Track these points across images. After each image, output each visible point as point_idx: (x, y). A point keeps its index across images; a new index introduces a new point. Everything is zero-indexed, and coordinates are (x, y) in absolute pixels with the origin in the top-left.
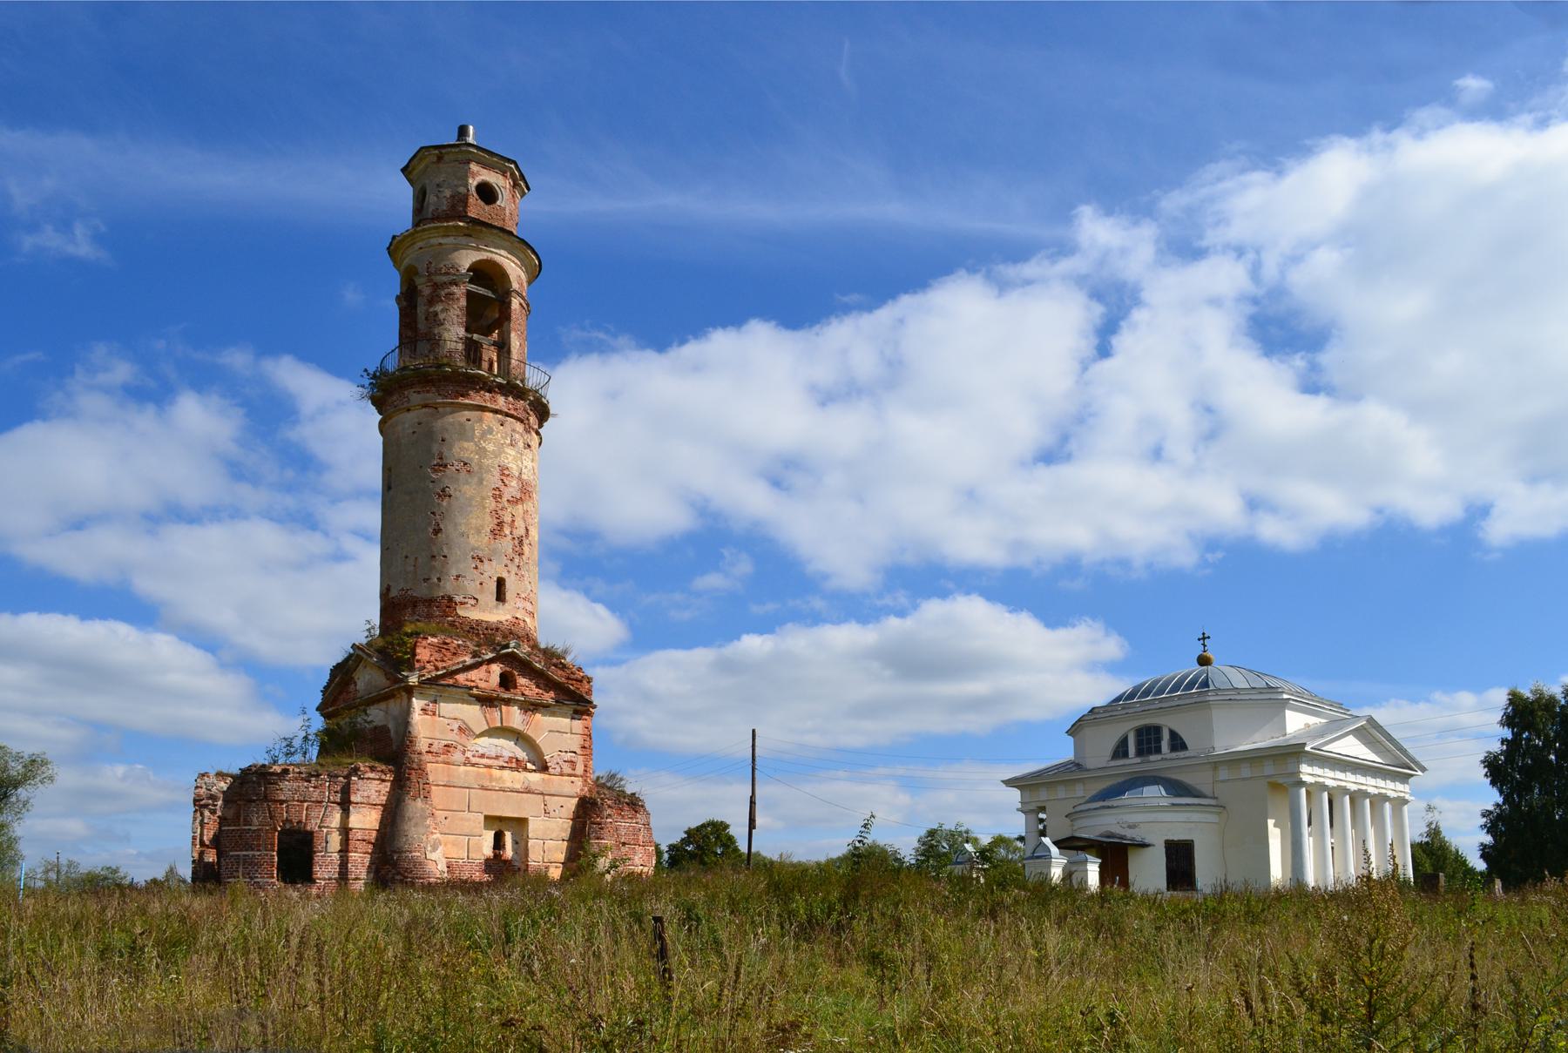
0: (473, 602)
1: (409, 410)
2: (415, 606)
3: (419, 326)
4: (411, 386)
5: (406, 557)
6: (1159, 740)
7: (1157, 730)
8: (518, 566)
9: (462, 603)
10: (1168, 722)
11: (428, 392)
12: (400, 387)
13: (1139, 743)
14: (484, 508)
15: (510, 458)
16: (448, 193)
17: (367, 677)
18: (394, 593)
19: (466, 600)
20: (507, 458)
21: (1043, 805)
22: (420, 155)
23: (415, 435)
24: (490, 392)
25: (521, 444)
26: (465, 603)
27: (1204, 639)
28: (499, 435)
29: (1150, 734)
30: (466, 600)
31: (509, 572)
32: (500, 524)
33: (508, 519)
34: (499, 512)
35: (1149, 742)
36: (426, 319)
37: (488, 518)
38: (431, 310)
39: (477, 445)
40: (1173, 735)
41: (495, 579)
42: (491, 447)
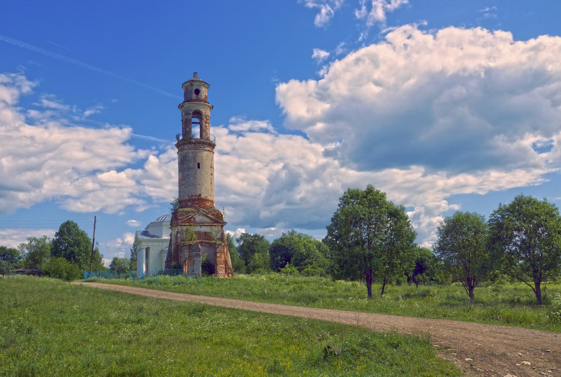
4: (206, 144)
11: (209, 147)
17: (201, 218)
21: (149, 247)
23: (207, 158)
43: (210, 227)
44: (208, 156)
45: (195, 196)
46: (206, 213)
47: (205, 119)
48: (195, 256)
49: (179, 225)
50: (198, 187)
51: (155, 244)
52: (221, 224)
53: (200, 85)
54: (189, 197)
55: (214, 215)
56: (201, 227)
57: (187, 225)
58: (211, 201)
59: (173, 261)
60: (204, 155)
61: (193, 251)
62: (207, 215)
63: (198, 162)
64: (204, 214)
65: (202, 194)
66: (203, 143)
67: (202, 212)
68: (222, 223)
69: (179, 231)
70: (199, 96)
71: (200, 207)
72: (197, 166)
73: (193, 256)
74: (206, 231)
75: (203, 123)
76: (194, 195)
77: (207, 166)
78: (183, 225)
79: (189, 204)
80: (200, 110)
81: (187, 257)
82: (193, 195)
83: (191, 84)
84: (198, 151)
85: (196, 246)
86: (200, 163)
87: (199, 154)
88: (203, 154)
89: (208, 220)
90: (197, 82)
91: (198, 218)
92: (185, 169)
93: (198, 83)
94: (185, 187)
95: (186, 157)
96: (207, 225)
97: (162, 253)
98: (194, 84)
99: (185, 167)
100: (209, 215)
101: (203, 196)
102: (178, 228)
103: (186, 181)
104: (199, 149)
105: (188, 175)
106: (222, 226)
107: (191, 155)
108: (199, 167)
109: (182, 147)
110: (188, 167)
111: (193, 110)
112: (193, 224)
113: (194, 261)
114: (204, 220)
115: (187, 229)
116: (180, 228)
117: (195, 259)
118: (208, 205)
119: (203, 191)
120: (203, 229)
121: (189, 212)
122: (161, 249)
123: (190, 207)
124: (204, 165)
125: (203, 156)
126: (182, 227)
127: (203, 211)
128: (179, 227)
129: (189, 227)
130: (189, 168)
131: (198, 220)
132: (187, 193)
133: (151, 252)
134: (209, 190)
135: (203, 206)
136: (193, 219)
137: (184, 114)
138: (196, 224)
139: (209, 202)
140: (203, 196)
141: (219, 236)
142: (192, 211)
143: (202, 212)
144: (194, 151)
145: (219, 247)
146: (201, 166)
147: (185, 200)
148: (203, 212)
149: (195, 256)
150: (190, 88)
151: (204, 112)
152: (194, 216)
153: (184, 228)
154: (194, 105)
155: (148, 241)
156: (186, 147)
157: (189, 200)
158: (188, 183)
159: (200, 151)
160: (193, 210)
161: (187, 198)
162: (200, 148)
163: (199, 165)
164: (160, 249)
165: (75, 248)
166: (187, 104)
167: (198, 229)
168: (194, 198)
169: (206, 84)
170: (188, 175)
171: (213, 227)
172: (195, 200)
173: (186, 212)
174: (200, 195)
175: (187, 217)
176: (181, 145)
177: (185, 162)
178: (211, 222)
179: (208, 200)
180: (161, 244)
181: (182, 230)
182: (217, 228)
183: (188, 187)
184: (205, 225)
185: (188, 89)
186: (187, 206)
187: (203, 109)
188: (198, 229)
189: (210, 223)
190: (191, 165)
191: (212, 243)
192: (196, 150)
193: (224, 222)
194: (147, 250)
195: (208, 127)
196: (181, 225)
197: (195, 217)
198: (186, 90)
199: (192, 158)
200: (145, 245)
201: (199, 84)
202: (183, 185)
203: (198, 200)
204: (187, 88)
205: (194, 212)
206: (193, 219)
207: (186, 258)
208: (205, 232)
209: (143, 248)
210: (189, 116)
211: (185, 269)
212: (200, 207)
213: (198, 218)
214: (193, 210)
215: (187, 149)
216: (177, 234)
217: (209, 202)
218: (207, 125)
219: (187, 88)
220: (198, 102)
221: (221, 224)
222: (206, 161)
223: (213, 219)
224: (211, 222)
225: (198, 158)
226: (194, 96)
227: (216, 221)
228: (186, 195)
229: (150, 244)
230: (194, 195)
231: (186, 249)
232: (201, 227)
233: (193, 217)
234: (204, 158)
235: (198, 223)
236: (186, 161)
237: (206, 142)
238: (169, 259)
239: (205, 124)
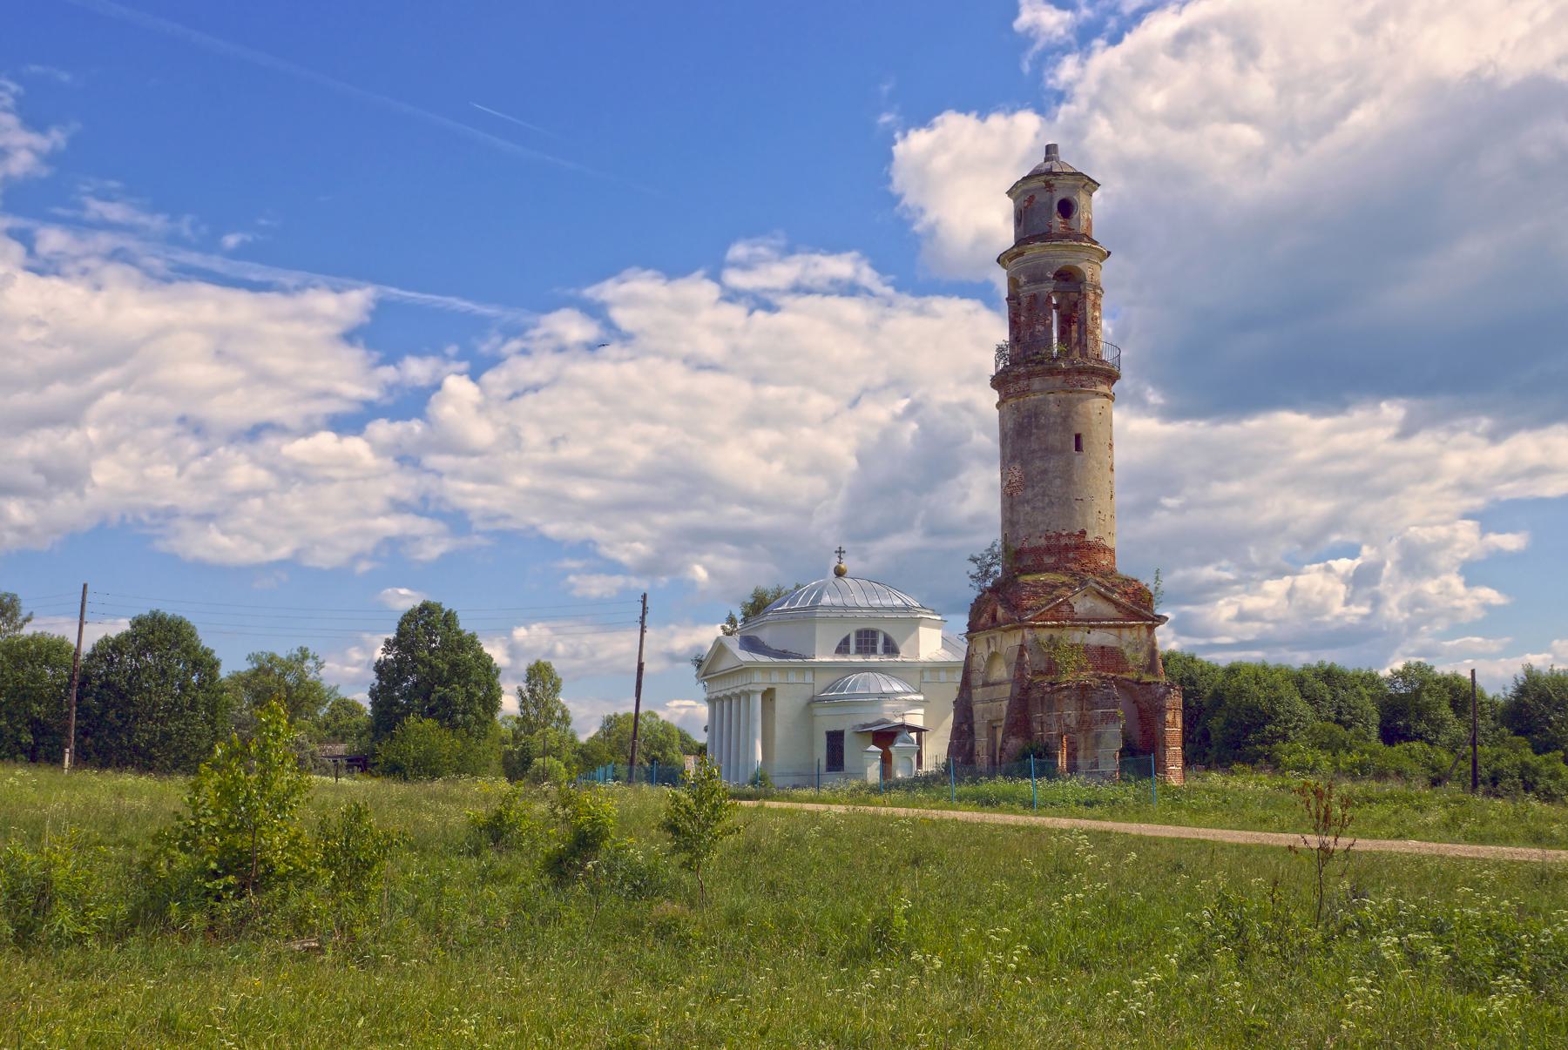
4: (1099, 375)
6: (874, 643)
7: (874, 633)
10: (884, 628)
11: (1105, 384)
13: (859, 642)
17: (1088, 605)
27: (840, 552)
29: (868, 636)
35: (866, 642)
40: (887, 641)
43: (1115, 631)
44: (1103, 414)
45: (1070, 535)
46: (1107, 588)
47: (1092, 296)
48: (1102, 720)
49: (1026, 626)
50: (1077, 508)
51: (793, 678)
52: (1150, 622)
53: (1075, 187)
54: (1048, 538)
55: (1126, 593)
56: (1089, 633)
57: (1052, 627)
59: (1013, 735)
60: (1093, 408)
61: (1096, 705)
62: (1109, 594)
63: (1078, 432)
64: (1099, 593)
65: (1088, 532)
66: (1093, 373)
67: (1094, 585)
68: (1153, 620)
69: (1028, 645)
70: (1073, 223)
71: (1084, 570)
72: (1073, 443)
73: (1096, 721)
74: (1103, 644)
75: (1088, 309)
76: (1064, 533)
77: (1101, 444)
78: (1039, 626)
79: (1049, 560)
80: (1080, 266)
81: (1074, 722)
82: (1061, 535)
83: (1047, 182)
84: (1076, 396)
85: (1106, 691)
86: (1084, 434)
87: (1080, 406)
88: (1090, 406)
89: (1109, 610)
90: (1066, 177)
91: (1083, 604)
92: (1034, 452)
93: (1070, 181)
94: (1034, 508)
95: (1036, 415)
96: (1109, 627)
97: (813, 705)
98: (1057, 183)
99: (1035, 446)
100: (1115, 596)
101: (1090, 537)
102: (1023, 636)
103: (1037, 489)
104: (1080, 392)
105: (1045, 472)
106: (1151, 629)
107: (1054, 409)
108: (1078, 447)
109: (1023, 383)
110: (1043, 447)
111: (1056, 269)
112: (1068, 623)
113: (1098, 736)
114: (1098, 611)
115: (1051, 638)
116: (1027, 633)
117: (1101, 728)
118: (1104, 562)
119: (1091, 520)
120: (1097, 638)
121: (1055, 587)
122: (810, 694)
123: (1054, 569)
124: (1096, 442)
125: (1091, 411)
126: (1037, 631)
127: (1098, 583)
128: (1026, 631)
129: (1056, 633)
130: (1048, 451)
131: (1082, 609)
132: (1042, 527)
133: (785, 706)
134: (1108, 517)
135: (1093, 566)
136: (1065, 607)
137: (1023, 279)
138: (1077, 622)
139: (1107, 555)
140: (1090, 537)
141: (1142, 656)
142: (1063, 584)
143: (1094, 585)
144: (1063, 395)
145: (1170, 693)
146: (1084, 442)
147: (1035, 551)
148: (1097, 586)
149: (1102, 720)
150: (1041, 198)
151: (1088, 273)
152: (1071, 596)
153: (1044, 635)
154: (1059, 251)
155: (767, 670)
156: (1036, 383)
157: (1048, 550)
158: (1044, 495)
159: (1082, 395)
160: (1065, 579)
161: (1043, 542)
162: (1082, 386)
163: (1078, 437)
164: (808, 692)
165: (454, 689)
166: (1035, 249)
167: (1078, 637)
168: (1063, 541)
169: (1091, 183)
170: (1045, 472)
171: (1126, 633)
172: (1067, 548)
173: (1045, 584)
174: (1083, 533)
175: (1053, 600)
176: (1017, 378)
177: (1034, 431)
178: (1120, 615)
179: (1105, 549)
180: (809, 678)
181: (1036, 640)
182: (1135, 633)
183: (1044, 508)
184: (1101, 627)
185: (1037, 198)
186: (1040, 569)
187: (1089, 265)
188: (1078, 637)
189: (1114, 619)
190: (1054, 439)
191: (1126, 680)
192: (1070, 395)
193: (1159, 617)
194: (769, 695)
196: (1032, 627)
197: (1071, 601)
198: (1026, 204)
199: (1059, 420)
200: (760, 681)
201: (1073, 182)
202: (1028, 502)
203: (1077, 548)
204: (1032, 197)
205: (1070, 587)
206: (1065, 607)
207: (1066, 725)
208: (1103, 647)
209: (754, 692)
210: (1044, 285)
211: (1062, 761)
212: (1084, 570)
213: (1083, 604)
214: (1065, 579)
215: (1041, 391)
216: (1021, 655)
217: (1107, 555)
218: (1097, 314)
219: (1032, 197)
220: (1075, 243)
221: (1150, 622)
222: (1100, 429)
223: (1124, 607)
224: (1120, 615)
225: (1075, 417)
226: (1057, 221)
227: (1133, 612)
228: (1039, 534)
229: (776, 678)
230: (1064, 533)
231: (1069, 699)
232: (1089, 633)
233: (1066, 602)
234: (1094, 417)
235: (1080, 620)
236: (1036, 427)
237: (1101, 369)
238: (965, 727)
239: (1091, 310)
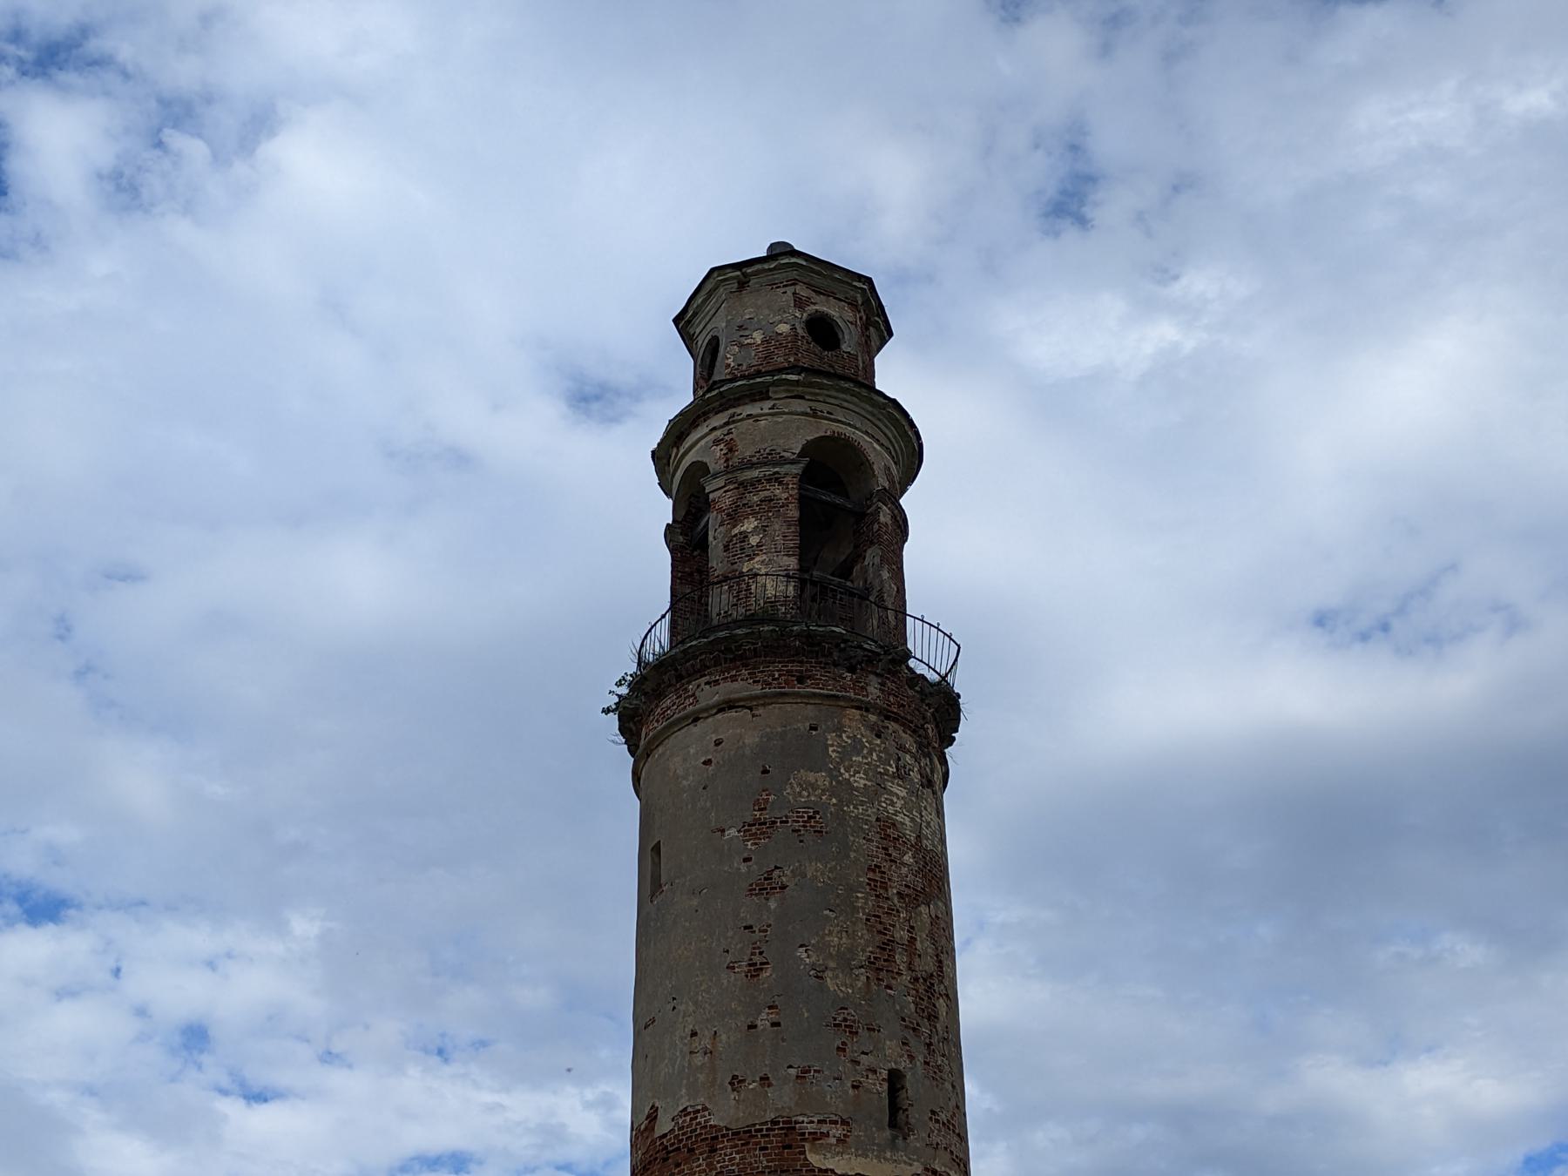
0: (837, 1131)
1: (696, 720)
2: (713, 1150)
3: (713, 563)
4: (700, 672)
5: (694, 1034)
8: (929, 1045)
9: (816, 1137)
11: (734, 679)
12: (680, 678)
14: (855, 910)
15: (899, 804)
16: (758, 337)
18: (664, 1126)
19: (824, 1128)
20: (893, 804)
22: (709, 286)
24: (852, 670)
25: (915, 776)
26: (828, 1135)
28: (875, 757)
30: (824, 1128)
31: (911, 1057)
32: (887, 946)
33: (902, 935)
34: (885, 919)
36: (726, 548)
37: (861, 931)
38: (736, 531)
39: (832, 777)
41: (885, 1074)
42: (860, 781)
58: (744, 1136)
179: (713, 1140)
195: (754, 540)
